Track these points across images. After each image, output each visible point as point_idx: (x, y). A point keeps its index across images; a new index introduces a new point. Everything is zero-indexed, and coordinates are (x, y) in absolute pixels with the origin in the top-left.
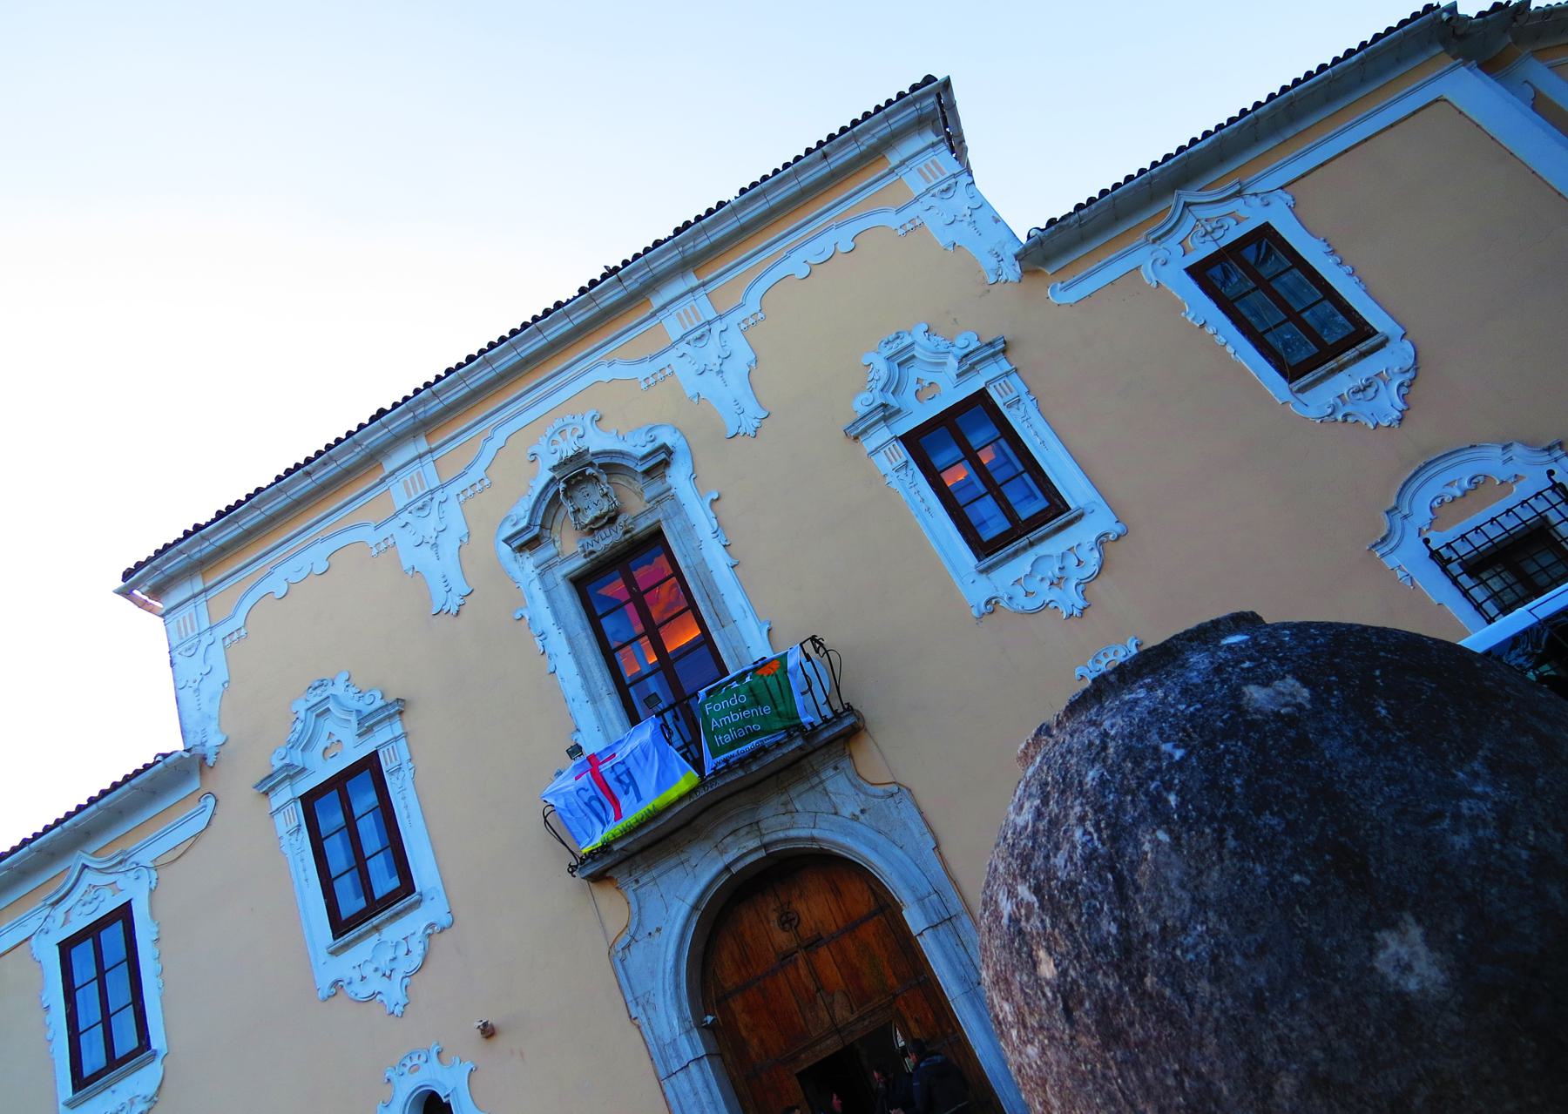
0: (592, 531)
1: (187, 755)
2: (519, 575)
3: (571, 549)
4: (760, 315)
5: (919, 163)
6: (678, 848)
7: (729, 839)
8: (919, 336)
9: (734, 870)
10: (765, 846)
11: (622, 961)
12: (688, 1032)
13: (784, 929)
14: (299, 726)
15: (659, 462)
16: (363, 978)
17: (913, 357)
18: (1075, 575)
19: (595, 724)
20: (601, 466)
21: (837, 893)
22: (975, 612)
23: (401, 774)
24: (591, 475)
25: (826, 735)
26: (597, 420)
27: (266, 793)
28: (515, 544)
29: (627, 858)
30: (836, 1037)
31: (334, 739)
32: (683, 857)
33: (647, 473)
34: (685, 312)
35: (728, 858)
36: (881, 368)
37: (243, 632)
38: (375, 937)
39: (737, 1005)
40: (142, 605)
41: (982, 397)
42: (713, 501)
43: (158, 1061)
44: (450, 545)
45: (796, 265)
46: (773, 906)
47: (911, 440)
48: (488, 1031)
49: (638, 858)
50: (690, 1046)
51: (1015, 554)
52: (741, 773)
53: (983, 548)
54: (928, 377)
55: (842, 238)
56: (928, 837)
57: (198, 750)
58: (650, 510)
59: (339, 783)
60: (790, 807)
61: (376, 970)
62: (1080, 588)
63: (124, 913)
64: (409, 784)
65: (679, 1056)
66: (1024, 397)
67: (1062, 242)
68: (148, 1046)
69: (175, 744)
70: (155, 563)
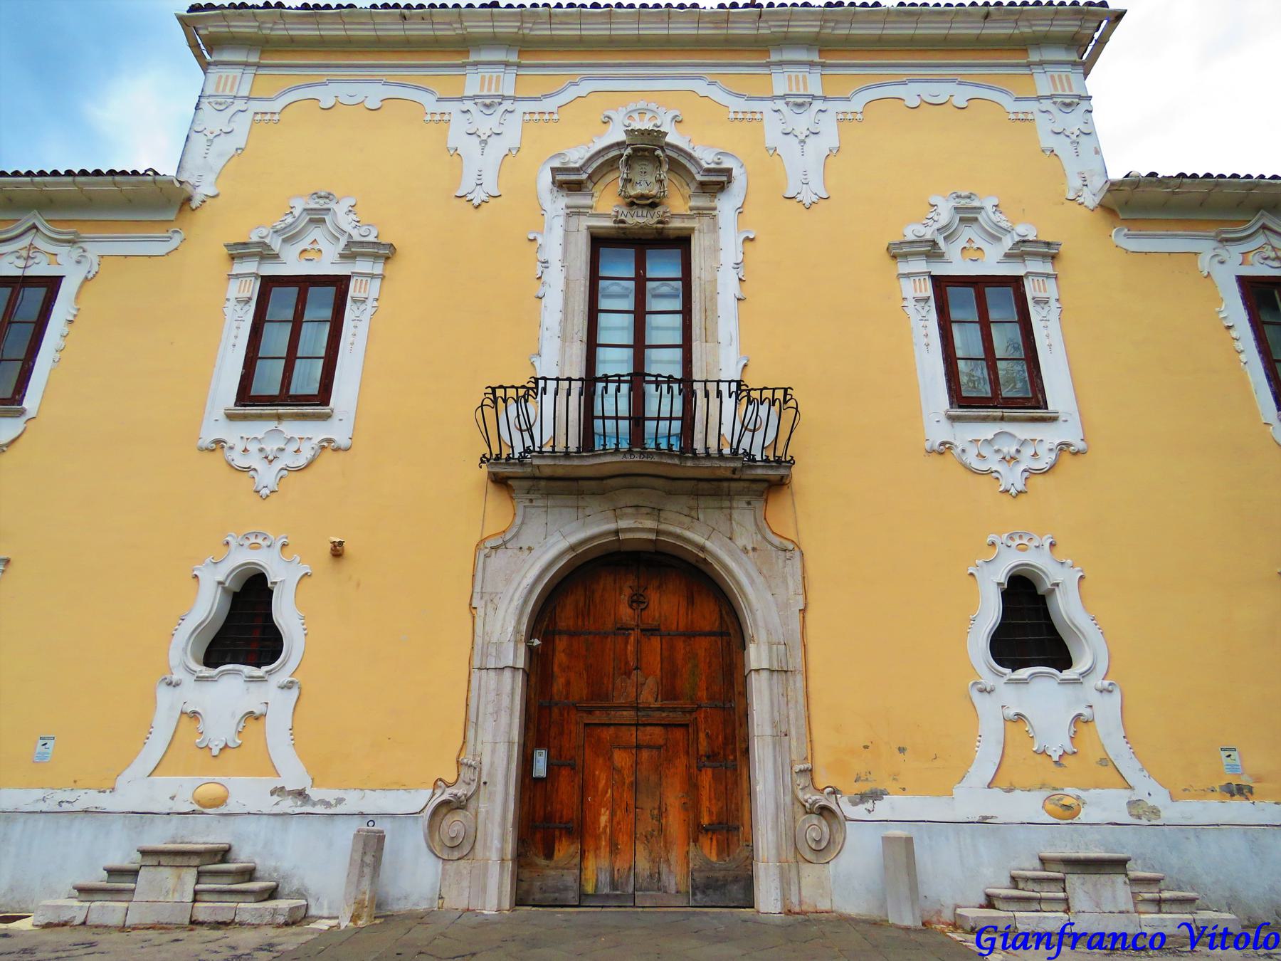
0: (631, 204)
1: (178, 185)
2: (547, 205)
3: (606, 206)
4: (859, 116)
5: (1055, 71)
6: (580, 493)
7: (629, 510)
8: (990, 209)
9: (622, 536)
10: (658, 532)
11: (487, 556)
12: (516, 643)
13: (631, 606)
14: (290, 220)
15: (717, 183)
16: (245, 450)
17: (976, 219)
18: (1026, 462)
19: (556, 358)
20: (667, 156)
21: (691, 601)
22: (928, 446)
23: (363, 307)
24: (658, 157)
25: (759, 472)
26: (677, 121)
27: (233, 258)
28: (559, 178)
29: (534, 478)
30: (633, 713)
31: (317, 247)
32: (581, 503)
33: (702, 184)
34: (797, 77)
35: (623, 524)
36: (945, 214)
37: (276, 117)
38: (272, 425)
39: (561, 644)
40: (194, 46)
41: (1016, 283)
42: (747, 239)
43: (24, 419)
44: (497, 149)
45: (910, 93)
46: (630, 583)
47: (941, 283)
48: (337, 551)
49: (543, 483)
50: (514, 655)
51: (985, 419)
52: (677, 461)
53: (961, 401)
54: (979, 242)
55: (961, 95)
56: (801, 598)
57: (189, 188)
58: (690, 217)
59: (304, 283)
60: (694, 514)
61: (261, 450)
62: (1026, 474)
63: (52, 285)
64: (366, 318)
65: (498, 657)
66: (1052, 302)
67: (1146, 203)
68: (20, 403)
69: (168, 169)
70: (225, 11)
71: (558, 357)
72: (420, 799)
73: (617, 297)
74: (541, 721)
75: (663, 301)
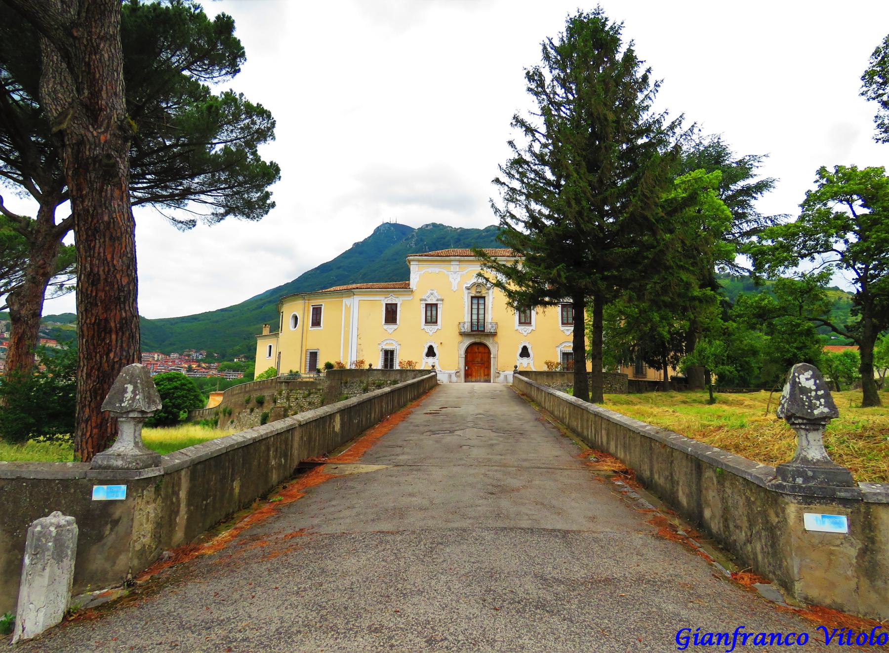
3: (473, 293)
44: (457, 281)
59: (432, 305)
71: (467, 319)
72: (454, 371)
73: (475, 306)
74: (466, 364)
75: (481, 307)
